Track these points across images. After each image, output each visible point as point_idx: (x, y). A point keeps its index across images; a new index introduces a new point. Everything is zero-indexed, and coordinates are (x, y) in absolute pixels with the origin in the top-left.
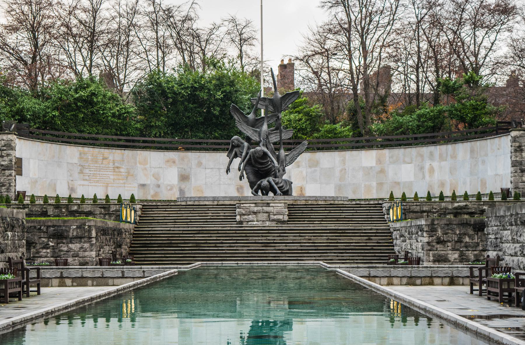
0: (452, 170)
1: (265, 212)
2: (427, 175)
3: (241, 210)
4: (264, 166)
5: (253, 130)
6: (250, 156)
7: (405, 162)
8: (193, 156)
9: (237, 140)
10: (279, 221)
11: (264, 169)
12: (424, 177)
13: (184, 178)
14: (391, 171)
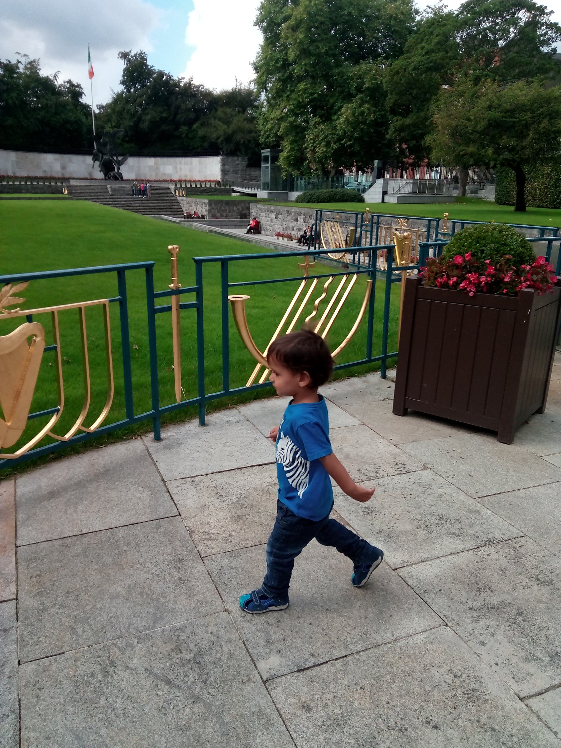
0: (190, 170)
2: (179, 172)
7: (168, 164)
8: (66, 157)
10: (128, 194)
12: (177, 172)
13: (64, 168)
14: (162, 168)
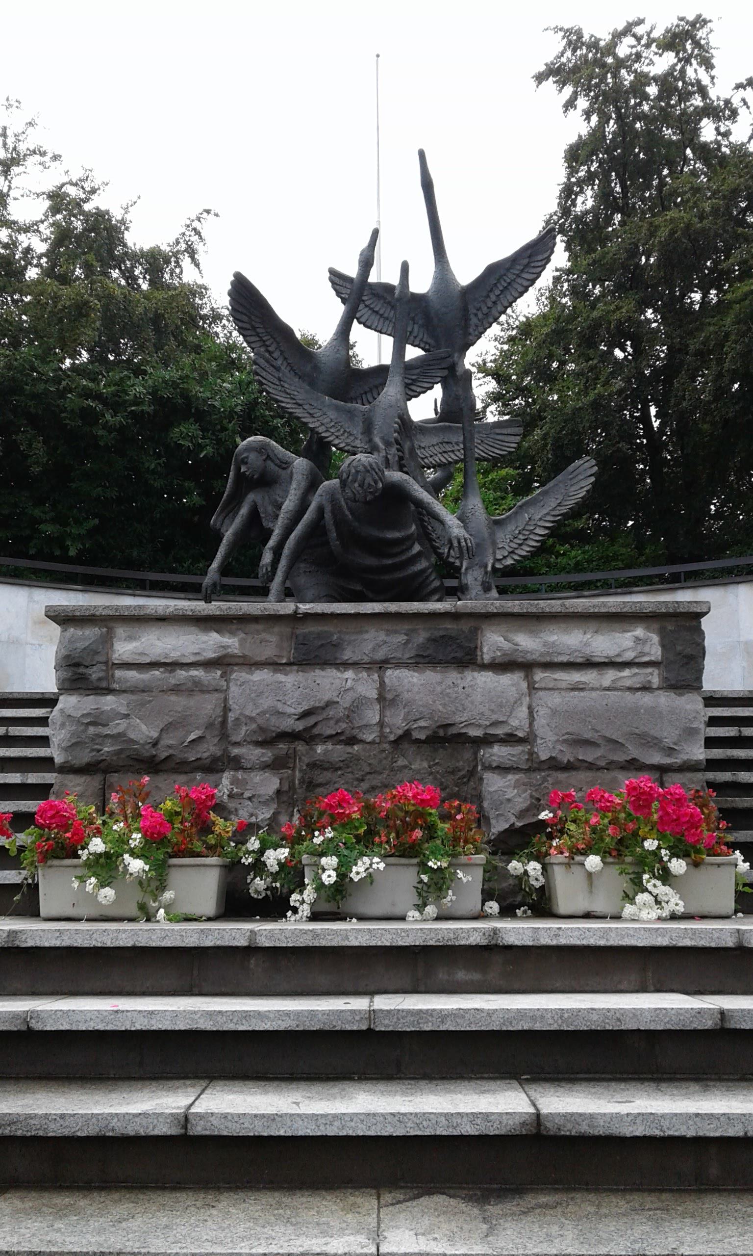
1: (422, 729)
3: (109, 702)
4: (389, 562)
5: (337, 408)
6: (321, 510)
9: (261, 449)
11: (386, 577)
